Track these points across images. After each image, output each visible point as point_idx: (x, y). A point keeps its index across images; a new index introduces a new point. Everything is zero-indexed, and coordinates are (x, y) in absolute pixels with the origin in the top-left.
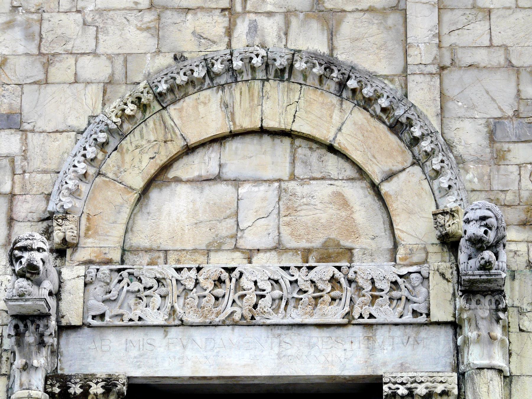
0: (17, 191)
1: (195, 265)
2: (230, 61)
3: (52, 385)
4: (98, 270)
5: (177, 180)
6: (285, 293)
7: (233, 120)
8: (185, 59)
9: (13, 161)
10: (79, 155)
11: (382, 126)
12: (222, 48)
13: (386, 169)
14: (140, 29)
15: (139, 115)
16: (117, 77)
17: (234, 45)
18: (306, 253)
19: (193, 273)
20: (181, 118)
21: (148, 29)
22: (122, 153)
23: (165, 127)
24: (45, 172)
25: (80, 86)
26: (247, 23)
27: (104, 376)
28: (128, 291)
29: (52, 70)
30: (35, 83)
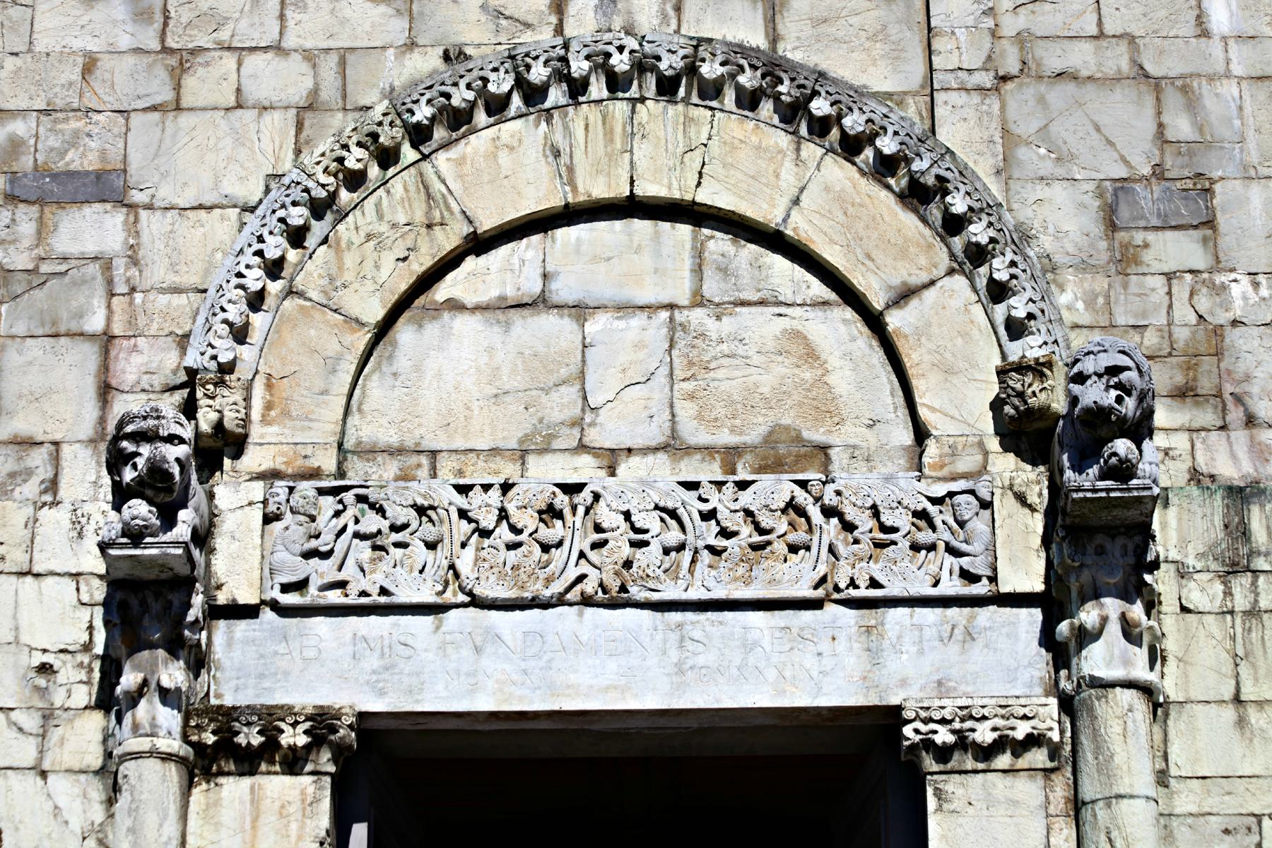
0: (117, 329)
2: (564, 60)
4: (291, 489)
5: (455, 306)
6: (690, 538)
7: (572, 183)
8: (468, 58)
12: (544, 36)
13: (896, 281)
15: (374, 171)
16: (325, 95)
17: (569, 31)
18: (730, 456)
19: (494, 496)
20: (461, 177)
22: (338, 250)
23: (429, 196)
25: (248, 115)
27: (310, 711)
28: (357, 535)
29: (189, 82)
30: (154, 108)
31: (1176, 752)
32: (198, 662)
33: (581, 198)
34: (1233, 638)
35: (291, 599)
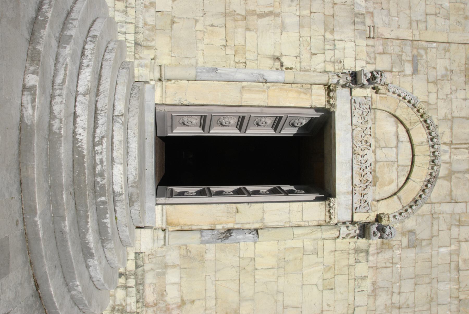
0: (393, 73)
1: (371, 134)
3: (333, 86)
5: (397, 127)
7: (417, 146)
9: (403, 71)
11: (415, 195)
14: (445, 114)
16: (430, 106)
18: (375, 171)
23: (415, 123)
24: (399, 83)
25: (427, 94)
26: (447, 149)
27: (336, 104)
29: (432, 84)
30: (428, 79)
31: (328, 241)
32: (343, 86)
33: (415, 147)
34: (345, 250)
35: (353, 101)
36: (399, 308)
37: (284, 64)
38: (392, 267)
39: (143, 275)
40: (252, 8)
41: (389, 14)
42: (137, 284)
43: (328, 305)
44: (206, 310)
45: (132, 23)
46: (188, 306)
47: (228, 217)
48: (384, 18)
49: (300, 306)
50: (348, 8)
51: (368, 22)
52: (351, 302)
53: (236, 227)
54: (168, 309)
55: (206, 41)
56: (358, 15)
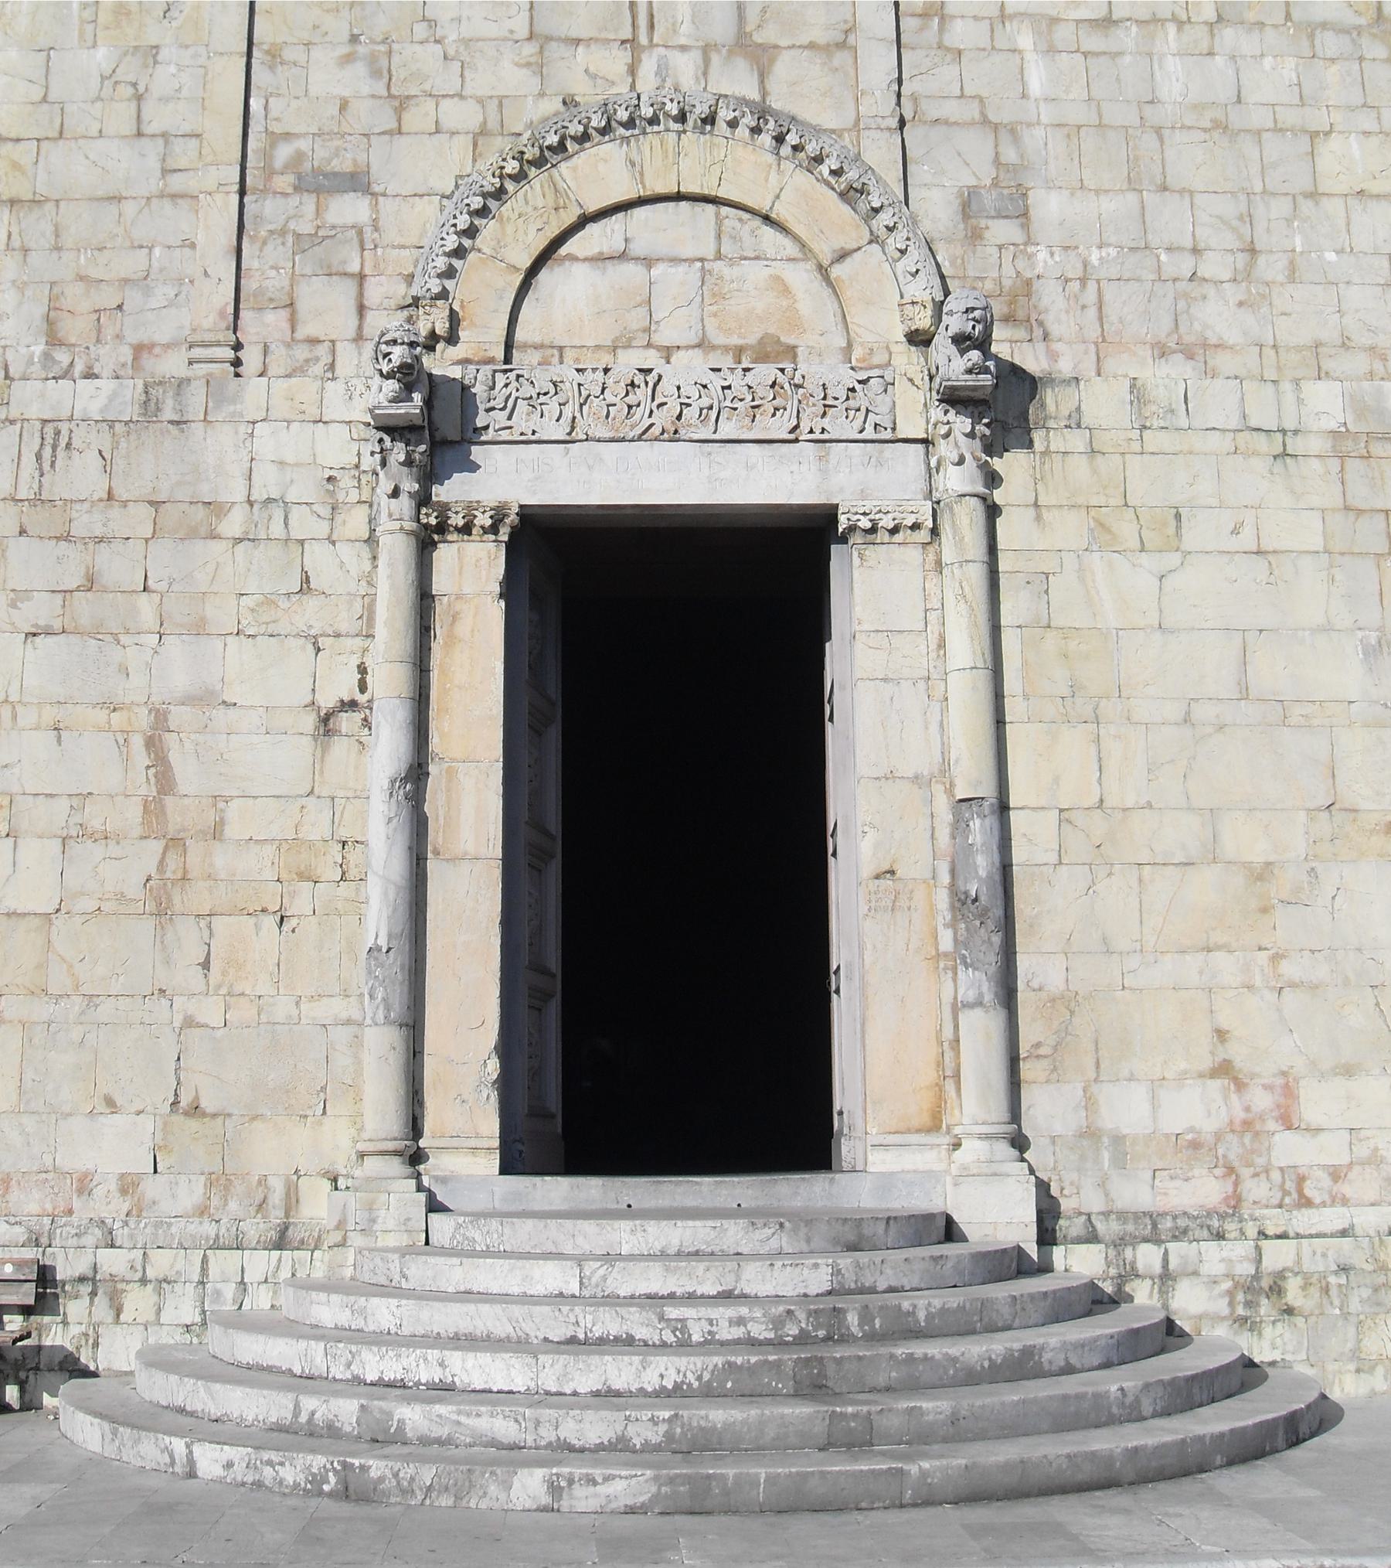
0: (367, 271)
1: (602, 366)
4: (478, 370)
8: (577, 105)
9: (360, 233)
10: (447, 226)
12: (624, 89)
13: (837, 246)
14: (517, 65)
17: (639, 88)
18: (738, 352)
21: (528, 65)
25: (444, 137)
26: (654, 59)
29: (406, 117)
30: (383, 133)
33: (648, 193)
34: (1034, 468)
36: (1252, 251)
37: (346, 699)
38: (1098, 281)
39: (1122, 1216)
40: (134, 813)
41: (143, 281)
42: (1155, 1239)
43: (1235, 531)
44: (1250, 987)
45: (205, 1260)
46: (1237, 1052)
47: (909, 909)
48: (154, 303)
49: (1238, 636)
50: (123, 444)
51: (173, 365)
52: (1225, 443)
53: (945, 878)
54: (1247, 1124)
55: (264, 987)
56: (149, 406)
